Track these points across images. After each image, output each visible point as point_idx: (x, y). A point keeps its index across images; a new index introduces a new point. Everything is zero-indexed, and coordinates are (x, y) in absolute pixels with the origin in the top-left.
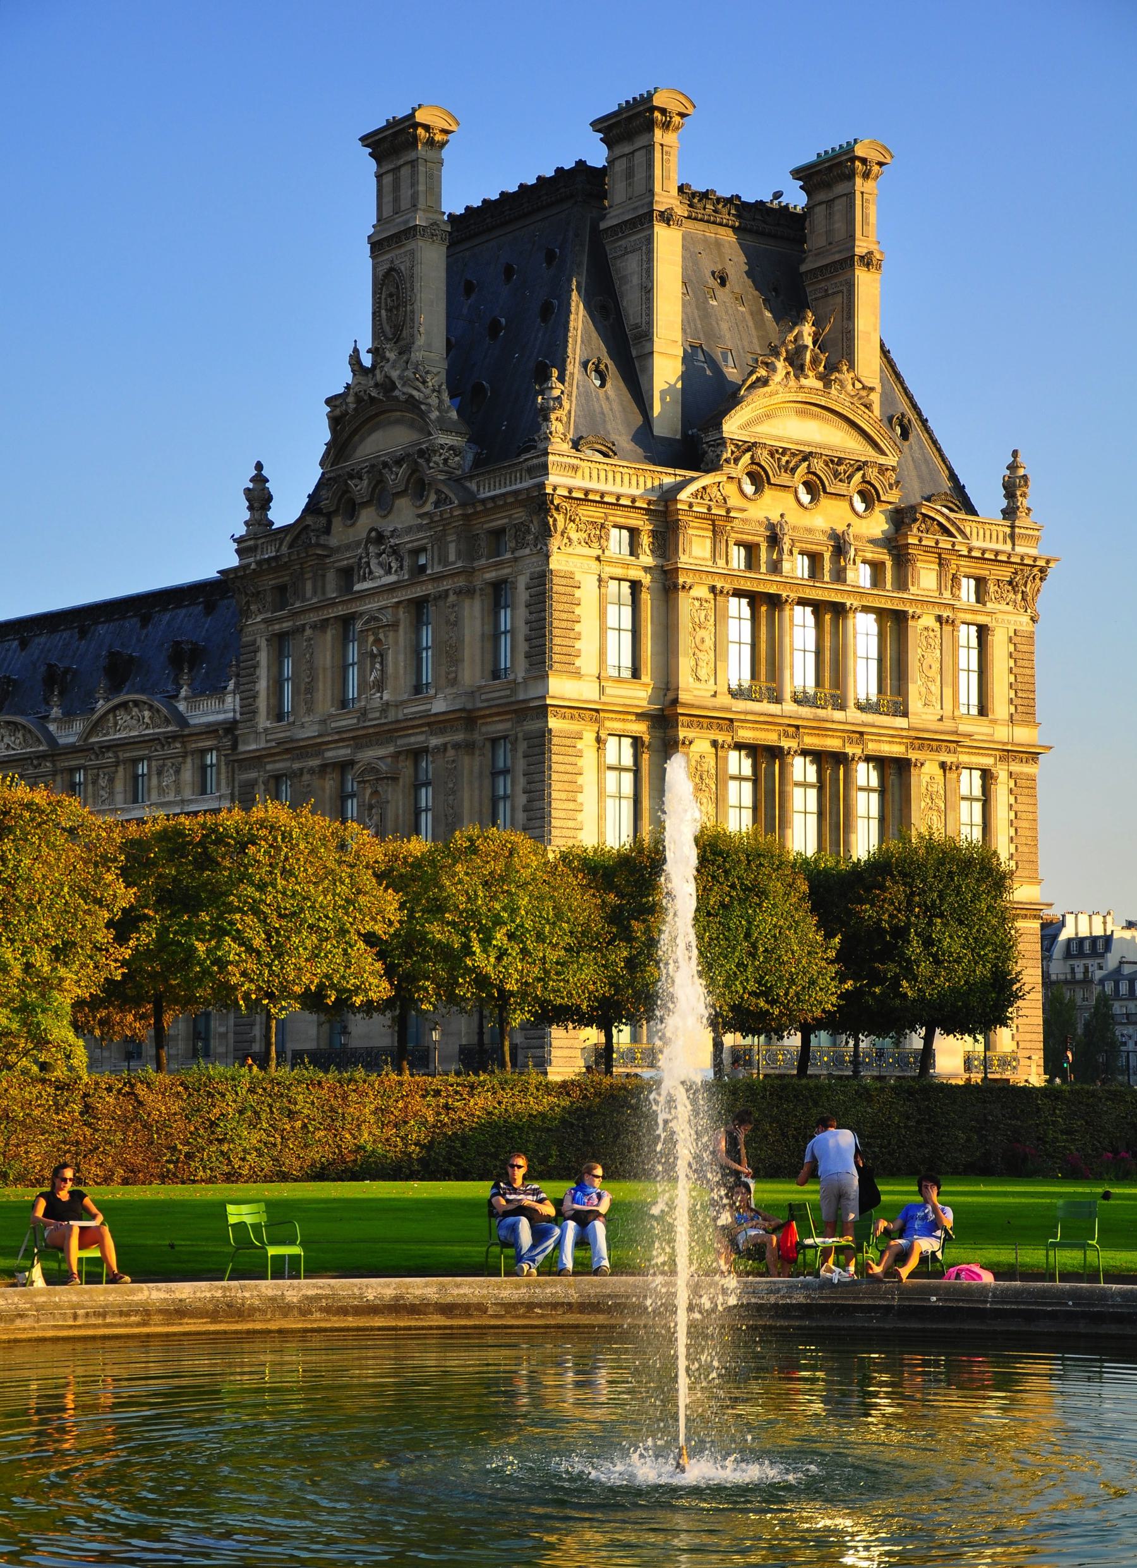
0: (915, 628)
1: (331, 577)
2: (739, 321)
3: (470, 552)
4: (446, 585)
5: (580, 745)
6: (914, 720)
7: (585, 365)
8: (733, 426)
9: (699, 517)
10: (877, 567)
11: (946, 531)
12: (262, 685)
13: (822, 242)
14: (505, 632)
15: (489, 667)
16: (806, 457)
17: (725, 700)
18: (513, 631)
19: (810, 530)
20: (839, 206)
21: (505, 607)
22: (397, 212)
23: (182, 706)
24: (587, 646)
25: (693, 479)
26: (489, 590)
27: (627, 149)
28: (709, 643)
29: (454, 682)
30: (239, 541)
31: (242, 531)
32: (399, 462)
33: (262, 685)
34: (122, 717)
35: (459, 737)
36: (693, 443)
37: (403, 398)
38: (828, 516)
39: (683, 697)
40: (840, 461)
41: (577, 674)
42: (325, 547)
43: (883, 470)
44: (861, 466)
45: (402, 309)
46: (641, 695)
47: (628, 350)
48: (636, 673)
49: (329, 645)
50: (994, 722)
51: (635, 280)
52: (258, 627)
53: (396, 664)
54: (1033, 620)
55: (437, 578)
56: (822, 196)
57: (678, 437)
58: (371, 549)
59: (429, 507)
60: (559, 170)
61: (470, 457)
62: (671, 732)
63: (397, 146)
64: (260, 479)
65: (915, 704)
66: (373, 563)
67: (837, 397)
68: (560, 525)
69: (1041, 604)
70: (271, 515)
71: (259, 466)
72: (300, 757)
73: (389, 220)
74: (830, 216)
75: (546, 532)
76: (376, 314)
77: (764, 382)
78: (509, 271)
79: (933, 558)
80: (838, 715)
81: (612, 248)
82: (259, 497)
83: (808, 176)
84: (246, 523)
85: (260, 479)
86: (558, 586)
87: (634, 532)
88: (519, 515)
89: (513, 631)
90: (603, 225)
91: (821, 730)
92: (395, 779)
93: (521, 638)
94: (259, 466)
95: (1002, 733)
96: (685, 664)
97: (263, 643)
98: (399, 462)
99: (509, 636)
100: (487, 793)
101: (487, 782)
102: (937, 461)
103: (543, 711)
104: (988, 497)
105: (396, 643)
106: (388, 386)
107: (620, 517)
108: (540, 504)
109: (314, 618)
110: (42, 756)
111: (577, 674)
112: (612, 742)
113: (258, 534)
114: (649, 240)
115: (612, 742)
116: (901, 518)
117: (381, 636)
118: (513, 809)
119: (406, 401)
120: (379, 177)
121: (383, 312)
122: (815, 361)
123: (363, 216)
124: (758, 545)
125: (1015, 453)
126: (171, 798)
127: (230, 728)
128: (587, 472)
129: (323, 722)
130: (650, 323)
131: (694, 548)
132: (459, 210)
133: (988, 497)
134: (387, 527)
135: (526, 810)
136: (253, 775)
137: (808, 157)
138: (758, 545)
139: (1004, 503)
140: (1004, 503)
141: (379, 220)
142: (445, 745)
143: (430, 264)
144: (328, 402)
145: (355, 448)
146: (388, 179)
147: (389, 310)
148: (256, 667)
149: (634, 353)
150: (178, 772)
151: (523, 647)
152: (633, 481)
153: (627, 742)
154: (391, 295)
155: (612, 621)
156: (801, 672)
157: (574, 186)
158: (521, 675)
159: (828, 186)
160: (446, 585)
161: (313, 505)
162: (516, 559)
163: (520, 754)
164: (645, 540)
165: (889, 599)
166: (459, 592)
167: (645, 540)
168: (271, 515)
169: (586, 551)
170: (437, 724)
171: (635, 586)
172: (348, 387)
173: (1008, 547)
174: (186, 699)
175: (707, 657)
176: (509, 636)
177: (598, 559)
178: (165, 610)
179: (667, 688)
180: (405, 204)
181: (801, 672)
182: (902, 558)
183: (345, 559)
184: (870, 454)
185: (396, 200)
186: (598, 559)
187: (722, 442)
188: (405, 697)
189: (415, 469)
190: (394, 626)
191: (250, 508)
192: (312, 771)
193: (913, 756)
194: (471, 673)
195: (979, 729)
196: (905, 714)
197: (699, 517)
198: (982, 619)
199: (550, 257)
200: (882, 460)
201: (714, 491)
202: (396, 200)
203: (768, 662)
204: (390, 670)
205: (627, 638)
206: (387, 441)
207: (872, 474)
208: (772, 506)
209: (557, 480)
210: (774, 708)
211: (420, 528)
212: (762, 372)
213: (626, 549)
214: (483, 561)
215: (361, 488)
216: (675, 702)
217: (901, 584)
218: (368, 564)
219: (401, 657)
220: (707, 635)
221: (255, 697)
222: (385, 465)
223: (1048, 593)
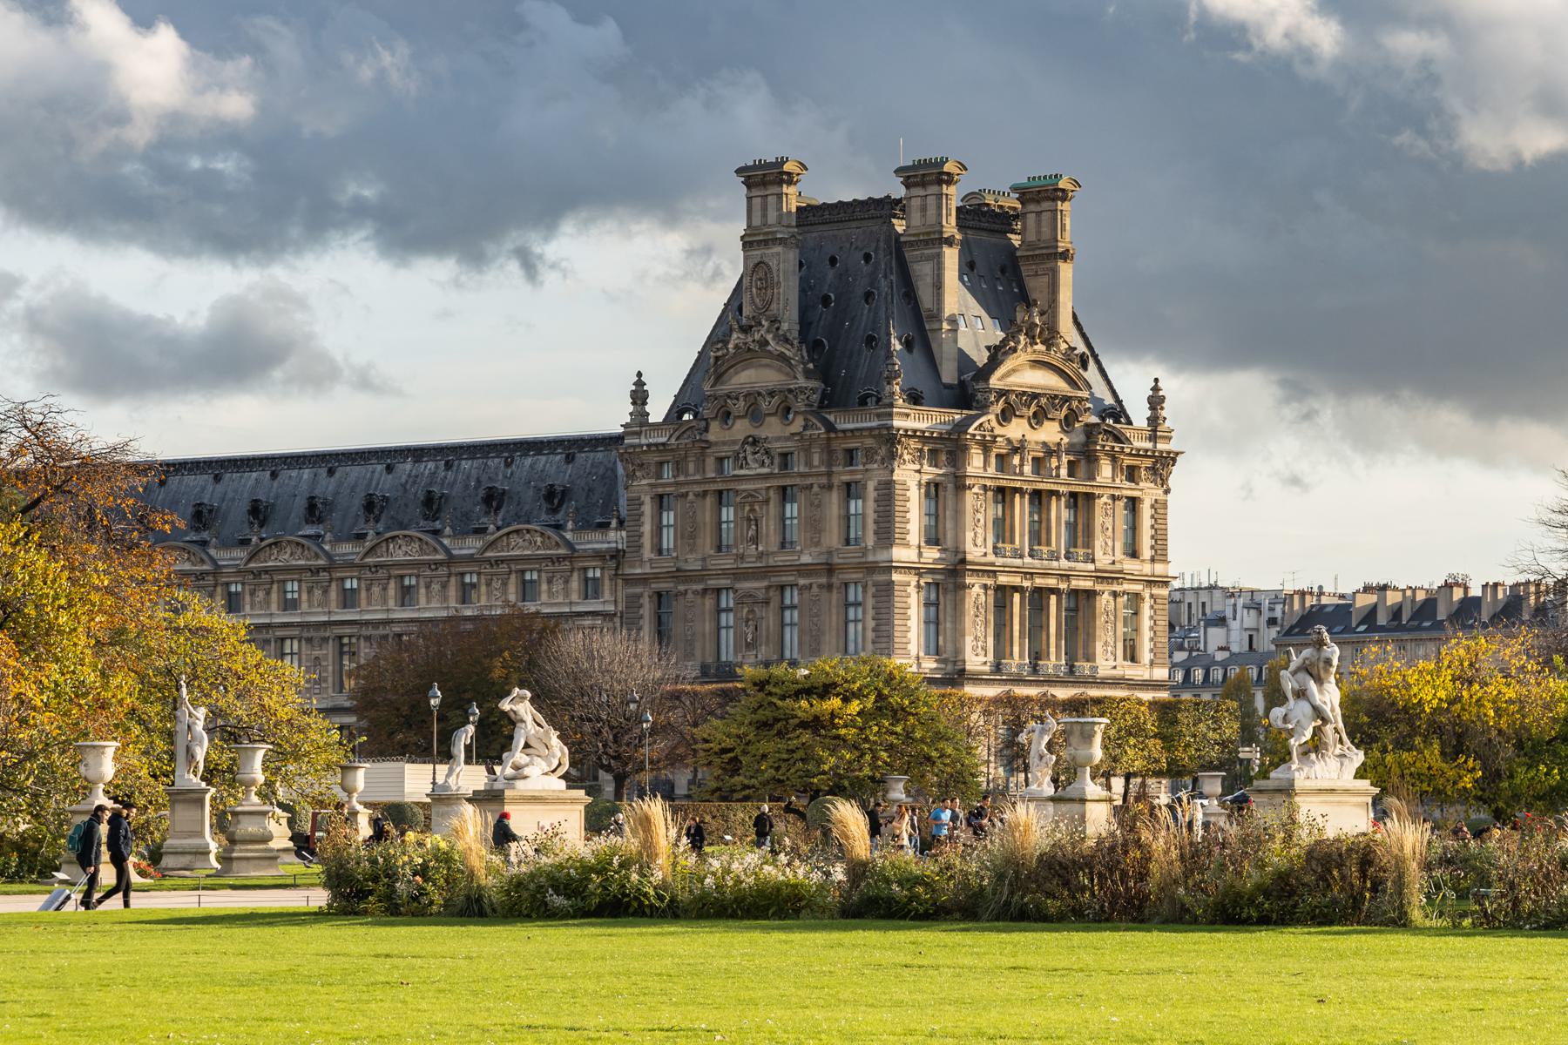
1: (710, 462)
5: (909, 589)
6: (1099, 565)
12: (647, 528)
15: (843, 536)
16: (1035, 396)
17: (991, 558)
20: (1046, 216)
23: (569, 536)
27: (921, 192)
29: (818, 544)
32: (771, 394)
33: (647, 528)
34: (514, 539)
35: (823, 580)
39: (969, 557)
41: (907, 545)
44: (1067, 399)
45: (769, 292)
51: (929, 280)
55: (802, 475)
56: (1032, 207)
58: (748, 448)
62: (960, 580)
64: (640, 383)
65: (1099, 554)
66: (750, 458)
67: (1055, 358)
69: (1171, 482)
71: (639, 374)
72: (685, 582)
74: (1039, 223)
75: (892, 456)
77: (1014, 350)
78: (833, 261)
80: (1055, 564)
81: (909, 255)
82: (639, 396)
85: (640, 383)
88: (869, 442)
92: (767, 603)
94: (639, 374)
95: (1147, 568)
97: (647, 499)
100: (842, 617)
101: (842, 610)
104: (1139, 414)
110: (438, 564)
111: (907, 545)
118: (864, 629)
120: (749, 199)
125: (1156, 380)
126: (560, 599)
127: (617, 556)
129: (704, 559)
131: (975, 463)
134: (762, 433)
135: (874, 630)
136: (638, 590)
139: (1149, 413)
140: (1149, 413)
141: (749, 226)
143: (784, 261)
146: (757, 202)
148: (642, 514)
150: (567, 582)
160: (809, 481)
163: (870, 594)
166: (822, 487)
170: (804, 570)
173: (1149, 445)
183: (725, 450)
185: (764, 216)
186: (919, 471)
190: (767, 501)
192: (695, 592)
193: (1098, 588)
195: (1130, 565)
196: (1093, 561)
199: (867, 257)
200: (1080, 394)
201: (986, 425)
207: (1075, 404)
208: (1017, 429)
210: (1018, 562)
211: (787, 439)
219: (772, 523)
221: (641, 536)
222: (759, 394)
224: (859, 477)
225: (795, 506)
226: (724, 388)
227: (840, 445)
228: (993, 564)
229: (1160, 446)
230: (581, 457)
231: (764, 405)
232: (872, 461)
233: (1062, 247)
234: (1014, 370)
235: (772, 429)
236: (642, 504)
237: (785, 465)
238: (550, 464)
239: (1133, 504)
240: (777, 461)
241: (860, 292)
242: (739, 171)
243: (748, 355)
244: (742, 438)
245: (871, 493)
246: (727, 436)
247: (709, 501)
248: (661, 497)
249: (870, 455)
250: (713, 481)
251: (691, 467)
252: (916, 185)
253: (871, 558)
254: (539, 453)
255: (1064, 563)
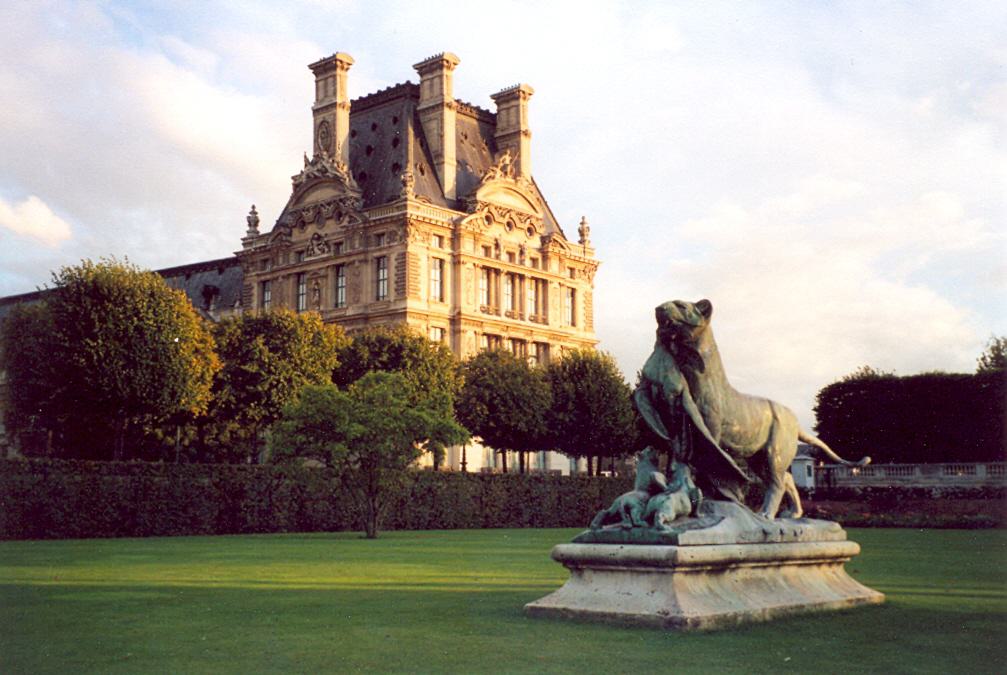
0: (551, 287)
2: (475, 155)
3: (366, 241)
4: (352, 259)
7: (416, 165)
8: (481, 195)
9: (469, 233)
10: (534, 261)
11: (562, 246)
13: (505, 125)
14: (384, 280)
18: (388, 279)
19: (510, 243)
20: (513, 110)
21: (383, 269)
22: (326, 96)
23: (211, 314)
24: (423, 287)
25: (465, 217)
26: (375, 261)
27: (430, 76)
28: (473, 287)
30: (243, 239)
31: (245, 235)
32: (329, 204)
36: (463, 202)
37: (331, 176)
38: (515, 238)
39: (463, 311)
40: (521, 214)
41: (419, 299)
42: (289, 241)
43: (538, 219)
46: (446, 310)
47: (432, 160)
48: (442, 300)
49: (291, 286)
50: (578, 330)
51: (435, 131)
52: (253, 279)
53: (326, 295)
54: (592, 287)
55: (350, 255)
56: (505, 106)
57: (455, 199)
58: (315, 242)
59: (345, 223)
60: (379, 92)
61: (362, 203)
62: (457, 327)
63: (326, 69)
64: (254, 213)
65: (551, 319)
66: (316, 249)
68: (413, 232)
70: (259, 229)
71: (253, 207)
73: (322, 101)
75: (406, 234)
76: (316, 141)
78: (374, 127)
79: (557, 258)
80: (522, 322)
81: (423, 118)
82: (253, 221)
83: (499, 98)
84: (248, 232)
85: (254, 213)
86: (410, 259)
87: (441, 238)
88: (393, 228)
89: (388, 279)
90: (418, 108)
91: (516, 329)
93: (392, 282)
94: (253, 207)
96: (463, 296)
97: (255, 285)
98: (329, 204)
99: (386, 282)
102: (552, 219)
103: (404, 314)
104: (573, 237)
105: (327, 284)
106: (324, 171)
107: (436, 231)
108: (403, 222)
109: (283, 273)
111: (419, 299)
112: (432, 330)
113: (253, 236)
114: (442, 114)
115: (432, 330)
116: (544, 240)
117: (319, 281)
119: (334, 178)
120: (317, 82)
121: (320, 140)
122: (511, 171)
123: (310, 99)
124: (490, 247)
125: (583, 218)
128: (424, 212)
130: (442, 149)
131: (467, 246)
132: (356, 98)
133: (573, 237)
134: (322, 233)
137: (497, 91)
138: (490, 247)
139: (579, 238)
140: (579, 238)
141: (317, 100)
142: (353, 330)
144: (293, 178)
145: (305, 199)
146: (321, 83)
147: (322, 139)
149: (435, 162)
151: (393, 286)
152: (445, 215)
153: (438, 331)
154: (324, 132)
155: (433, 277)
156: (506, 304)
157: (405, 93)
158: (392, 299)
159: (508, 101)
160: (352, 259)
161: (279, 224)
162: (390, 247)
164: (446, 242)
165: (539, 273)
166: (360, 261)
167: (446, 242)
168: (259, 229)
169: (421, 244)
171: (442, 261)
172: (302, 172)
174: (214, 310)
175: (472, 294)
176: (386, 282)
177: (428, 248)
178: (197, 272)
179: (456, 307)
180: (330, 93)
181: (506, 304)
182: (545, 258)
184: (532, 212)
185: (326, 91)
187: (476, 202)
188: (330, 309)
189: (338, 207)
190: (326, 277)
191: (250, 225)
193: (551, 342)
194: (367, 297)
197: (469, 233)
198: (574, 286)
199: (395, 120)
200: (537, 215)
201: (475, 222)
202: (326, 91)
203: (492, 297)
204: (324, 296)
205: (438, 284)
206: (323, 194)
207: (534, 221)
208: (496, 231)
209: (411, 212)
210: (498, 318)
212: (491, 174)
213: (437, 245)
214: (373, 248)
215: (309, 215)
216: (459, 313)
217: (545, 268)
218: (313, 249)
219: (329, 291)
220: (472, 284)
222: (322, 205)
223: (598, 277)
224: (384, 252)
225: (344, 279)
226: (301, 206)
227: (373, 232)
228: (480, 317)
229: (588, 257)
230: (228, 270)
231: (324, 210)
232: (394, 240)
233: (523, 128)
234: (493, 193)
235: (331, 229)
236: (252, 288)
237: (337, 251)
238: (211, 278)
239: (573, 291)
240: (332, 248)
241: (389, 141)
242: (311, 67)
243: (316, 181)
244: (310, 236)
245: (393, 263)
246: (303, 237)
247: (292, 280)
248: (264, 283)
249: (392, 236)
250: (294, 267)
251: (281, 260)
252: (426, 73)
253: (392, 307)
254: (205, 270)
255: (527, 323)
